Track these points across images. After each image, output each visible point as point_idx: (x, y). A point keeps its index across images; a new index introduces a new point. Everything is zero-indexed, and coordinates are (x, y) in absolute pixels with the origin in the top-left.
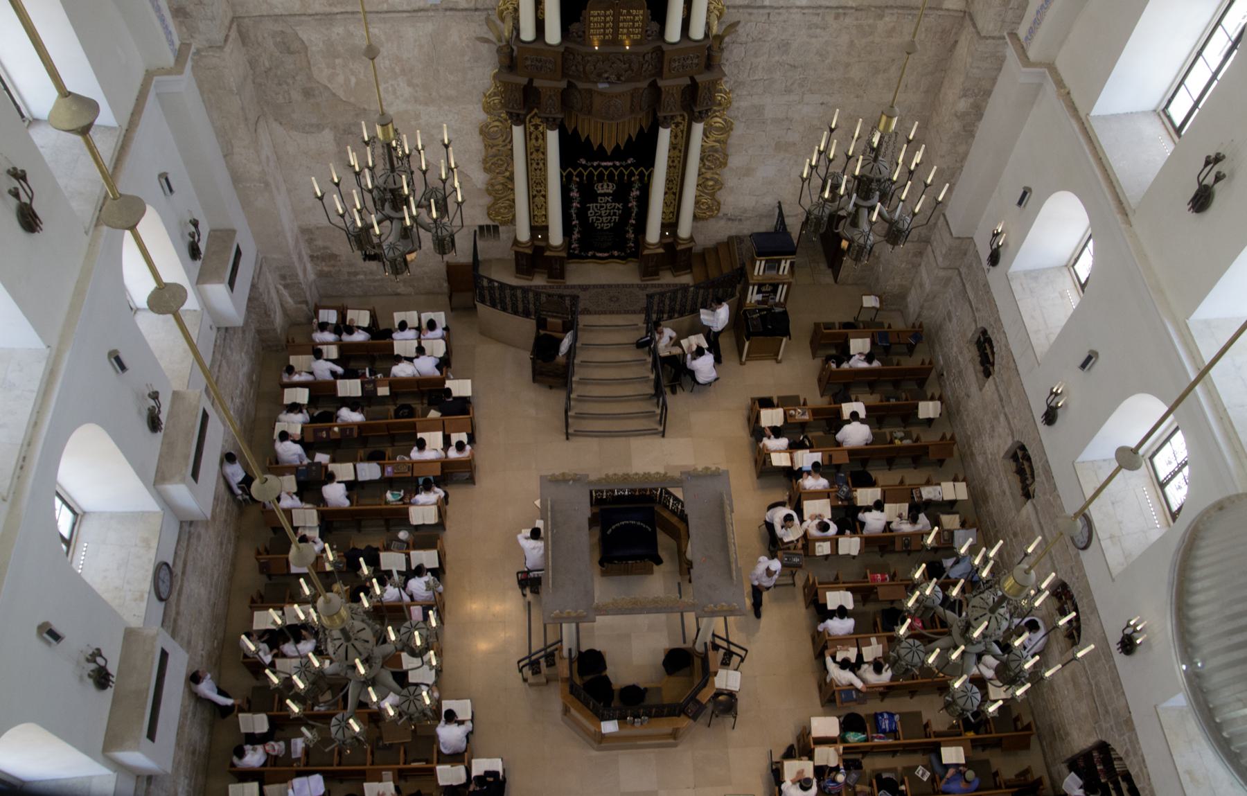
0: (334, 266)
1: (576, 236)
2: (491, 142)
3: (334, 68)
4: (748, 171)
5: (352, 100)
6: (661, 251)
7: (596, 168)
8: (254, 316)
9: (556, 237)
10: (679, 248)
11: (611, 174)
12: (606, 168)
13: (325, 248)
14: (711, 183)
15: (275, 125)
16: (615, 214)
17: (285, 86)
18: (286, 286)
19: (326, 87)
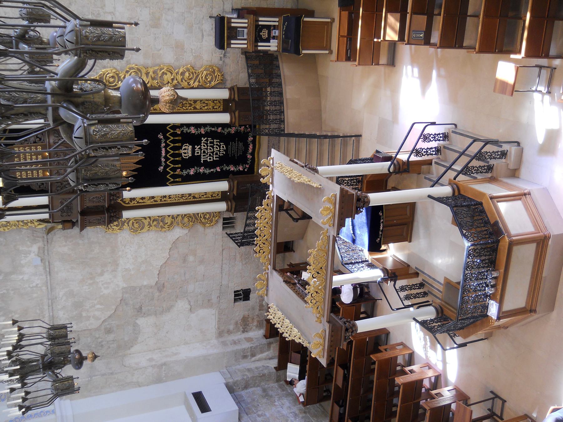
0: (253, 319)
1: (232, 168)
2: (146, 227)
3: (89, 317)
4: (179, 47)
5: (114, 307)
6: (237, 113)
7: (167, 159)
8: (263, 384)
9: (223, 186)
10: (236, 98)
11: (173, 148)
12: (167, 152)
13: (236, 323)
14: (187, 74)
15: (133, 350)
16: (212, 143)
17: (103, 343)
18: (253, 355)
19: (104, 321)
